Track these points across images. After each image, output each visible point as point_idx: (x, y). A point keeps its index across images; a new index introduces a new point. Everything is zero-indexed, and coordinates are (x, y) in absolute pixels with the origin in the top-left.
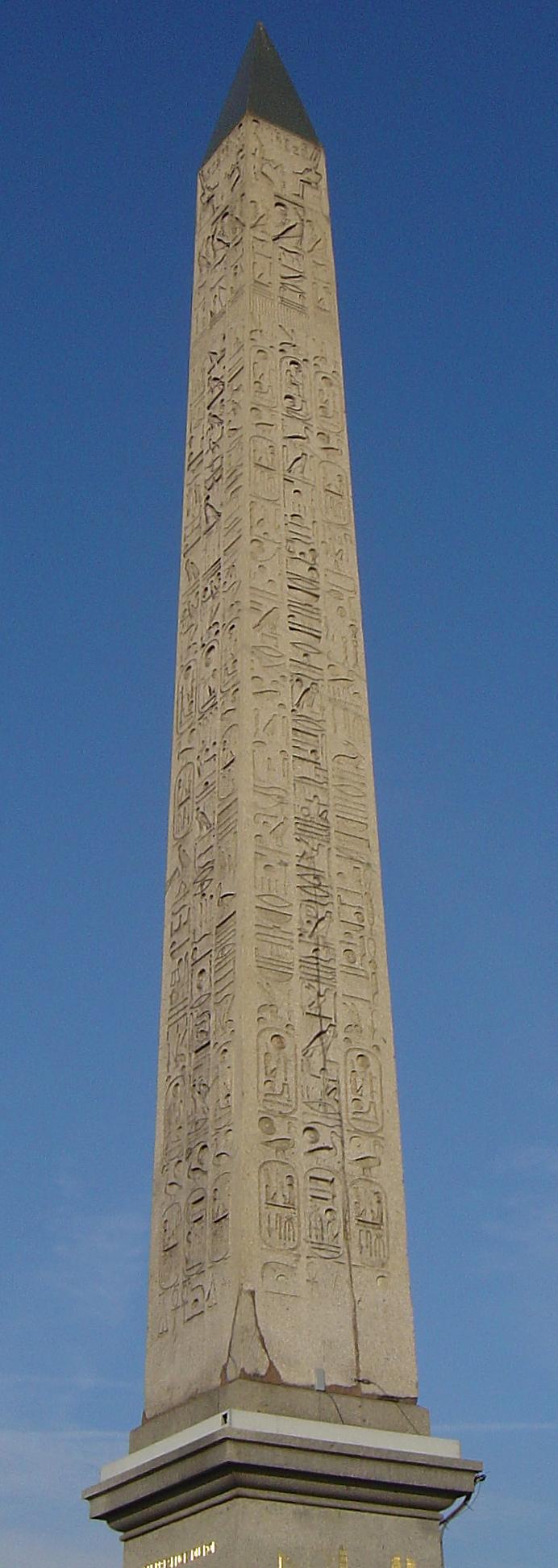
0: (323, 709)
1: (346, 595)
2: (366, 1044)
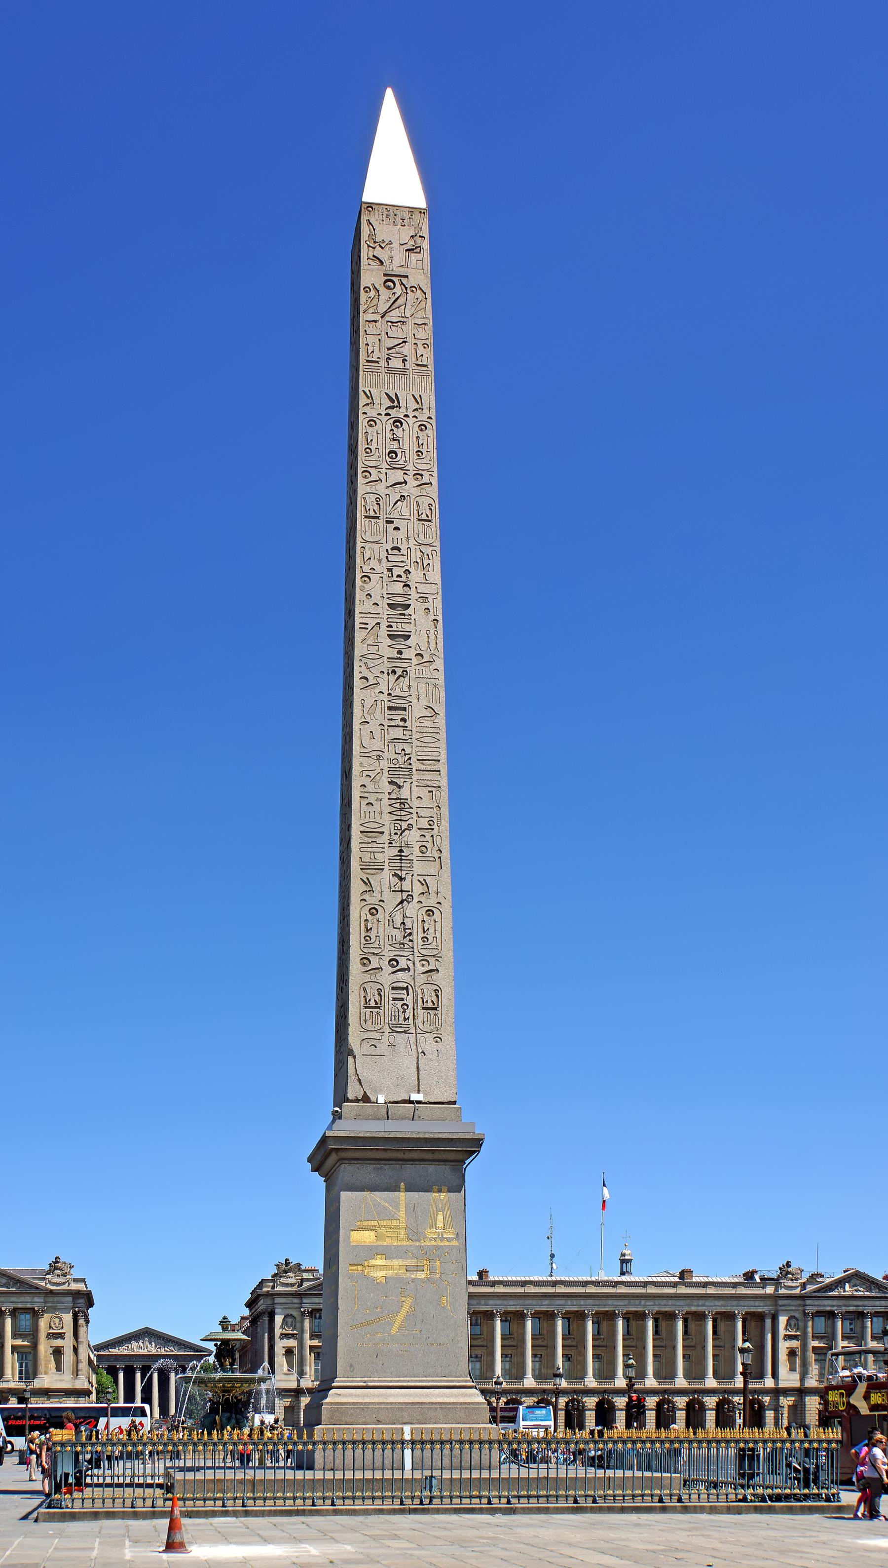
0: (409, 687)
1: (430, 597)
2: (431, 901)
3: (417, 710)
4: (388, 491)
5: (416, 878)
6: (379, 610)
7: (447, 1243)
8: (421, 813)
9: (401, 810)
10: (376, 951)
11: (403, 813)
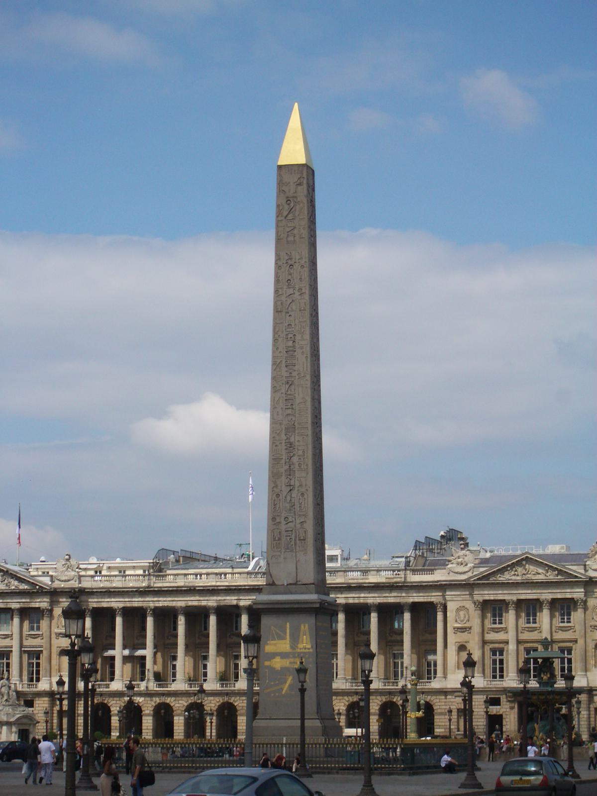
0: (295, 390)
1: (305, 347)
2: (303, 490)
3: (298, 401)
4: (287, 299)
5: (296, 478)
6: (282, 354)
7: (308, 651)
8: (300, 448)
9: (290, 447)
10: (279, 514)
11: (291, 449)
